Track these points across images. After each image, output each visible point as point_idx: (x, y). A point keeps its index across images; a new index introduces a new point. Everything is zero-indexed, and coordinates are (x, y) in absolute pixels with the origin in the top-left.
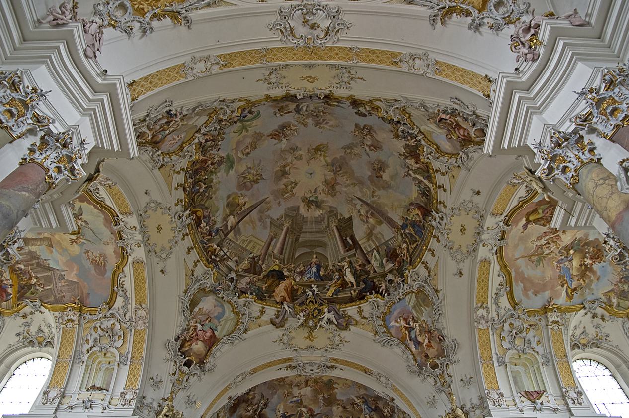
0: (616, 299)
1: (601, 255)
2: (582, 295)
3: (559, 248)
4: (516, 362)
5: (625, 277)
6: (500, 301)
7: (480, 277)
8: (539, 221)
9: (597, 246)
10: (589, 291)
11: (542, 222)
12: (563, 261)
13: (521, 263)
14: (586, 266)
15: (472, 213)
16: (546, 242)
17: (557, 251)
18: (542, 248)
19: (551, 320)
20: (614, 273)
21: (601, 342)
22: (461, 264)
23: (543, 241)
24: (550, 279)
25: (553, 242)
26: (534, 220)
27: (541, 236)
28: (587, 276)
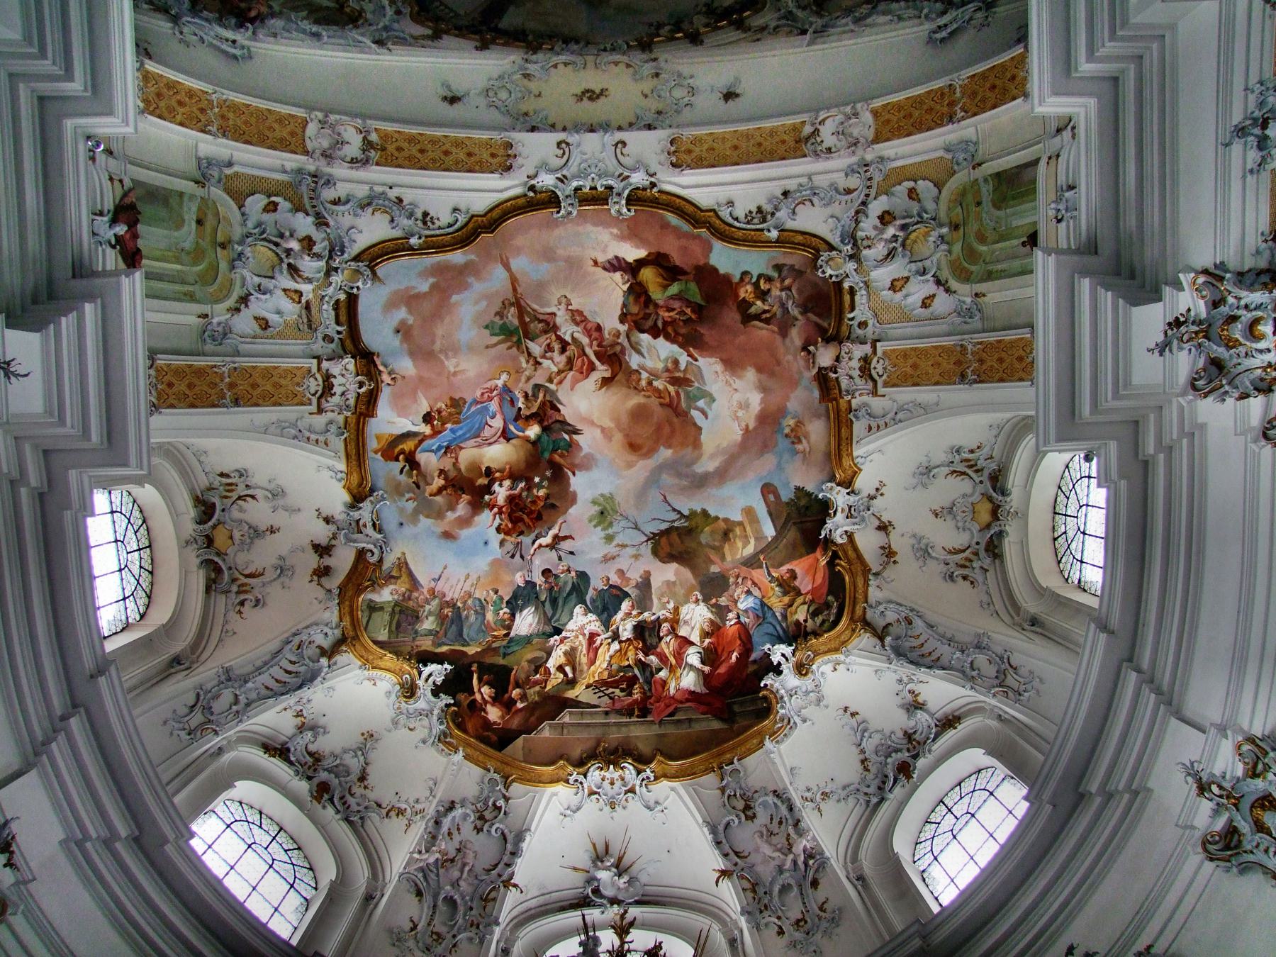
0: (390, 599)
1: (523, 528)
2: (398, 491)
3: (550, 380)
4: (210, 222)
5: (459, 616)
6: (377, 214)
7: (458, 143)
8: (637, 300)
9: (553, 506)
11: (634, 309)
12: (507, 405)
13: (496, 279)
14: (488, 489)
15: (654, 105)
16: (568, 338)
17: (540, 378)
18: (546, 332)
19: (335, 368)
20: (469, 583)
21: (228, 592)
22: (482, 102)
23: (568, 330)
24: (452, 370)
25: (570, 362)
26: (640, 284)
27: (585, 320)
28: (454, 499)
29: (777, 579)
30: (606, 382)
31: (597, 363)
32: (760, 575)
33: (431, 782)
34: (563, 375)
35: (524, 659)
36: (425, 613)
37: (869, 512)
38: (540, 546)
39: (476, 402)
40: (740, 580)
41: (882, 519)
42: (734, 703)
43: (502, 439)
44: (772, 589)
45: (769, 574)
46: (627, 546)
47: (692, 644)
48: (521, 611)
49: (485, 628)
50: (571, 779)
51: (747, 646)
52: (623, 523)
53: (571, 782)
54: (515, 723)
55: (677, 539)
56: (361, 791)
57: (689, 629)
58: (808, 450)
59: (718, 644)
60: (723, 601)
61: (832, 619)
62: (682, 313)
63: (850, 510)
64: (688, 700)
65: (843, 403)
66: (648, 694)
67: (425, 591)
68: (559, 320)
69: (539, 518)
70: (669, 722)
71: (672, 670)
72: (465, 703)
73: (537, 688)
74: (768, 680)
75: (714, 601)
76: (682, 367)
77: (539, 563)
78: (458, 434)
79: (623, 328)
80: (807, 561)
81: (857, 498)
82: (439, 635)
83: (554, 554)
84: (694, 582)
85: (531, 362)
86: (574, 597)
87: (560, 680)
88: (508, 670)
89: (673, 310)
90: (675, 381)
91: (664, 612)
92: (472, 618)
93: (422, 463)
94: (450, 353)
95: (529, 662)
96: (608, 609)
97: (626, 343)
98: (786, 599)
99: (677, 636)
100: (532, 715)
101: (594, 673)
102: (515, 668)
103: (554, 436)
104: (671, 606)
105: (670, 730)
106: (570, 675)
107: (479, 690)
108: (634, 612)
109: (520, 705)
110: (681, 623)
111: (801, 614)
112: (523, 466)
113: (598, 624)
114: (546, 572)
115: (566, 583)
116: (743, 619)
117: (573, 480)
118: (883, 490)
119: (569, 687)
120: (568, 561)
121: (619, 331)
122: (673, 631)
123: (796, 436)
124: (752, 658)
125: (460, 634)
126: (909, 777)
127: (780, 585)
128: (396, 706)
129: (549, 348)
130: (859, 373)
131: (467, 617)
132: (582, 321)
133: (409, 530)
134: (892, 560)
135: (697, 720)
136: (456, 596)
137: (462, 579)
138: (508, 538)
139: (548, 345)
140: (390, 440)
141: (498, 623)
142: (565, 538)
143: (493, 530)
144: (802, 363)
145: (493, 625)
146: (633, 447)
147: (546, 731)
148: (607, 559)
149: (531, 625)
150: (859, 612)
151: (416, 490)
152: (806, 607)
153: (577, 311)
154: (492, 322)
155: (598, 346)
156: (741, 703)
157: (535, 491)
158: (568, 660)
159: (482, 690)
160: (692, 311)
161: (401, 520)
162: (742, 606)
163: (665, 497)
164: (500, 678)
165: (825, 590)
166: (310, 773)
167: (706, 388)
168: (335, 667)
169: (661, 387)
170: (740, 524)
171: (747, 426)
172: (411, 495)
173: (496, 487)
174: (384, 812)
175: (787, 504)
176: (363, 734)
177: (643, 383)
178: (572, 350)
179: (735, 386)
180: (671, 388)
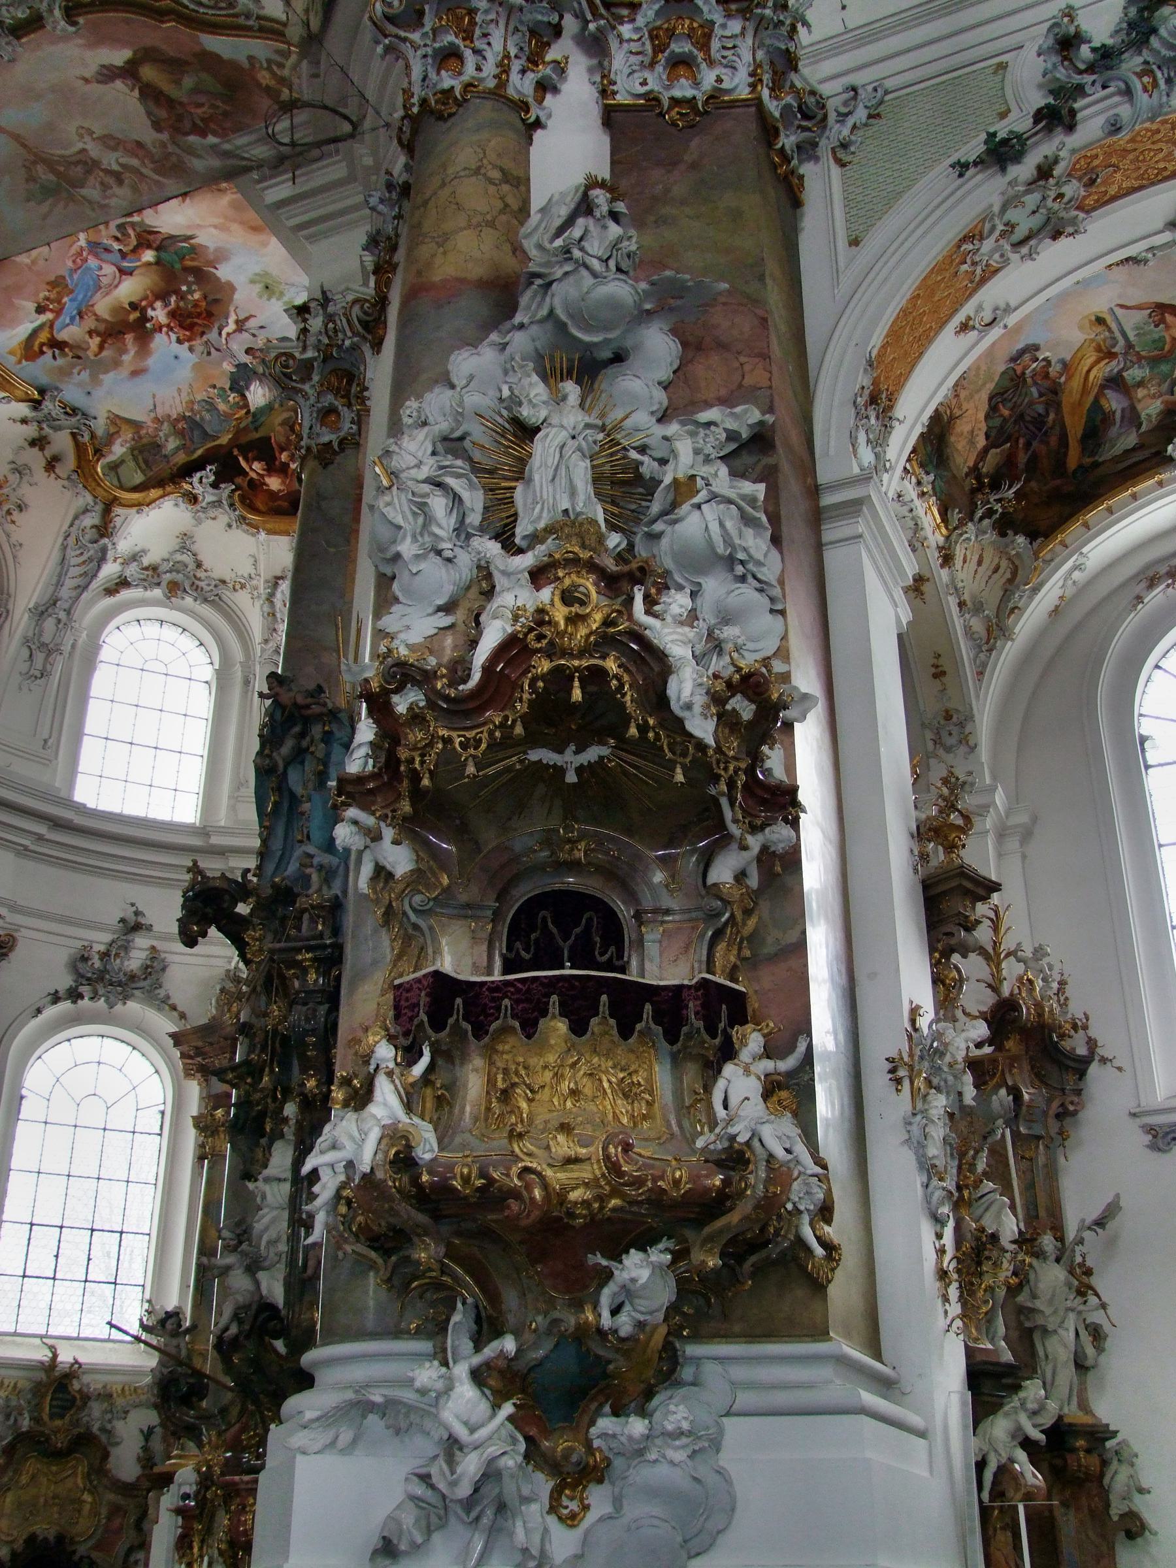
2: (65, 373)
9: (216, 301)
14: (144, 319)
16: (115, 167)
20: (184, 394)
23: (111, 160)
52: (293, 290)
69: (210, 315)
72: (245, 485)
83: (245, 335)
92: (207, 417)
95: (282, 424)
103: (172, 249)
109: (293, 466)
117: (219, 273)
125: (205, 433)
131: (202, 419)
133: (98, 393)
136: (180, 410)
142: (247, 319)
143: (175, 345)
164: (264, 450)
166: (156, 580)
173: (150, 313)
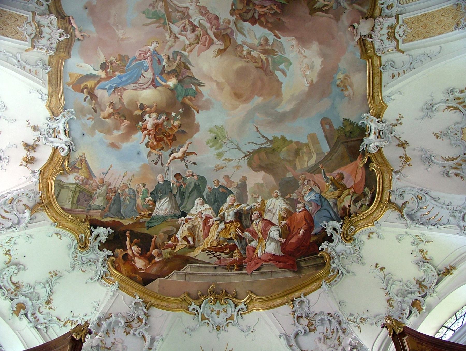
1: (163, 145)
3: (185, 50)
5: (119, 199)
9: (184, 132)
10: (89, 126)
11: (240, 6)
12: (156, 64)
14: (141, 118)
16: (196, 23)
17: (177, 47)
18: (182, 19)
20: (126, 178)
23: (196, 19)
24: (121, 37)
25: (198, 38)
27: (207, 12)
29: (331, 180)
30: (221, 52)
31: (215, 40)
32: (319, 178)
33: (96, 303)
34: (193, 46)
35: (161, 231)
36: (97, 195)
37: (392, 135)
38: (174, 158)
39: (135, 59)
40: (306, 182)
41: (401, 139)
42: (302, 261)
43: (151, 86)
44: (327, 186)
45: (325, 177)
46: (231, 160)
47: (273, 224)
48: (160, 200)
49: (136, 209)
50: (191, 308)
51: (310, 225)
52: (229, 145)
53: (190, 309)
54: (154, 270)
55: (265, 156)
56: (48, 310)
57: (271, 215)
58: (352, 94)
59: (291, 223)
60: (294, 196)
61: (367, 203)
62: (271, 9)
63: (379, 133)
64: (270, 260)
65: (376, 61)
66: (244, 256)
67: (97, 180)
68: (191, 12)
69: (174, 139)
70: (258, 274)
71: (260, 241)
73: (169, 250)
74: (324, 245)
75: (288, 196)
76: (271, 43)
77: (173, 169)
78: (123, 80)
79: (233, 18)
80: (351, 166)
81: (384, 125)
82: (105, 210)
84: (275, 184)
85: (173, 36)
86: (195, 192)
87: (185, 246)
88: (150, 237)
89: (265, 7)
90: (265, 52)
91: (255, 204)
92: (128, 202)
93: (98, 96)
94: (120, 27)
95: (164, 233)
96: (218, 201)
97: (234, 28)
98: (337, 193)
99: (263, 219)
100: (165, 266)
101: (207, 242)
102: (155, 236)
104: (260, 199)
105: (258, 278)
106: (192, 243)
107: (131, 248)
108: (235, 204)
109: (157, 259)
110: (266, 211)
111: (346, 203)
112: (164, 105)
113: (211, 211)
114: (178, 175)
115: (190, 183)
116: (307, 208)
117: (197, 116)
118: (402, 120)
119: (190, 250)
120: (192, 168)
121: (229, 20)
122: (261, 216)
123: (344, 86)
124: (313, 232)
125: (120, 211)
126: (420, 310)
127: (333, 184)
128: (74, 256)
129: (184, 29)
130: (386, 36)
131: (124, 200)
132: (206, 13)
134: (408, 163)
135: (277, 272)
136: (117, 186)
137: (122, 175)
138: (153, 151)
139: (184, 27)
140: (78, 78)
141: (145, 206)
142: (191, 153)
143: (143, 145)
144: (348, 36)
145: (141, 207)
146: (237, 95)
147: (174, 277)
148: (218, 168)
149: (166, 209)
150: (386, 197)
151: (94, 113)
152: (350, 197)
153: (203, 7)
154: (148, 10)
155: (216, 29)
156: (306, 261)
157: (172, 121)
158: (190, 233)
159: (132, 248)
160: (277, 8)
161: (85, 133)
162: (307, 199)
163: (257, 129)
165: (363, 184)
167: (286, 56)
168: (35, 220)
169: (256, 56)
170: (307, 145)
171: (312, 81)
172: (91, 116)
173: (147, 117)
174: (62, 323)
175: (338, 130)
176: (50, 273)
177: (245, 53)
178: (199, 31)
179: (304, 54)
180: (263, 56)
